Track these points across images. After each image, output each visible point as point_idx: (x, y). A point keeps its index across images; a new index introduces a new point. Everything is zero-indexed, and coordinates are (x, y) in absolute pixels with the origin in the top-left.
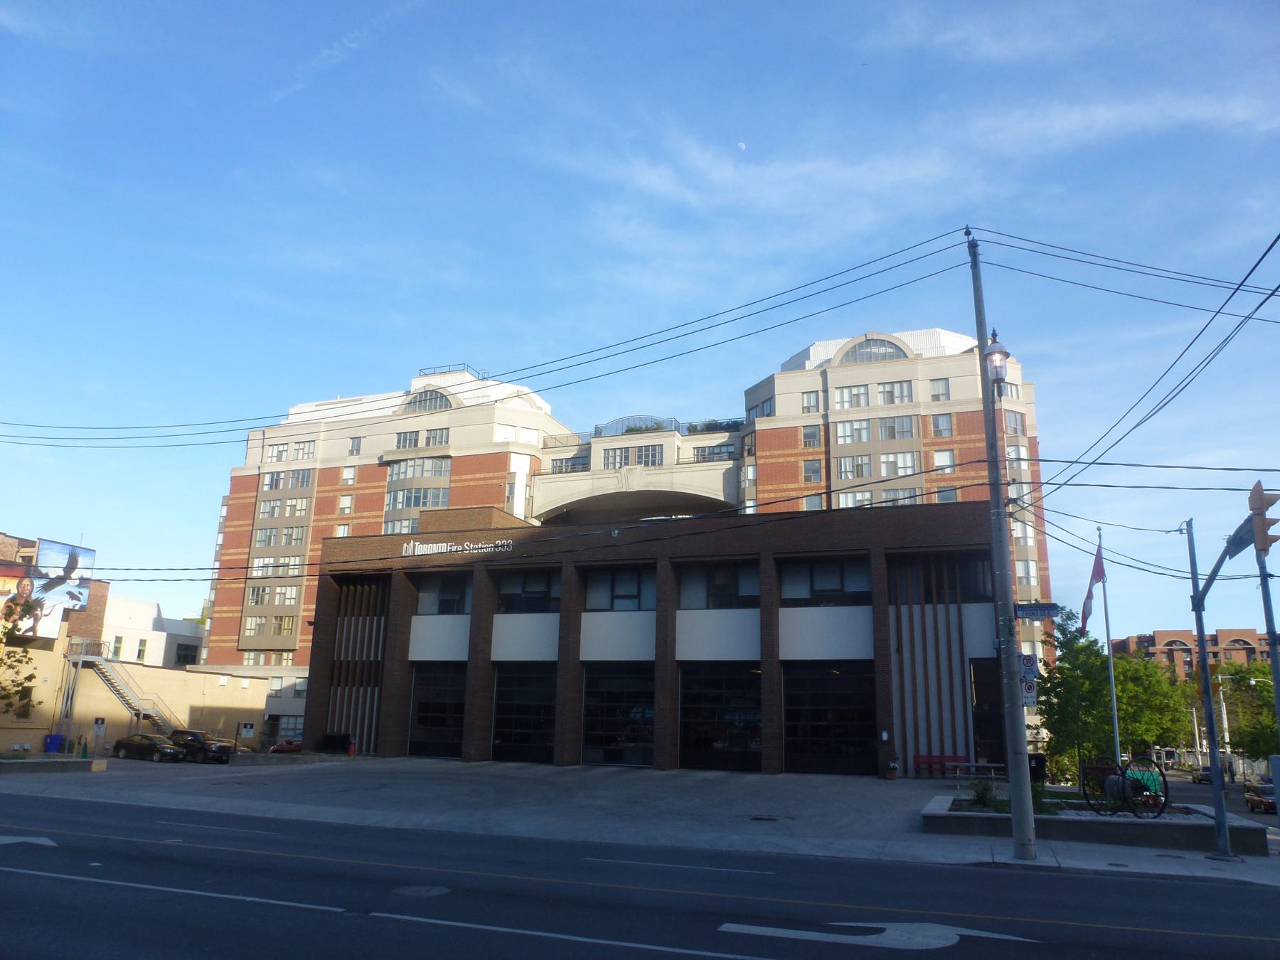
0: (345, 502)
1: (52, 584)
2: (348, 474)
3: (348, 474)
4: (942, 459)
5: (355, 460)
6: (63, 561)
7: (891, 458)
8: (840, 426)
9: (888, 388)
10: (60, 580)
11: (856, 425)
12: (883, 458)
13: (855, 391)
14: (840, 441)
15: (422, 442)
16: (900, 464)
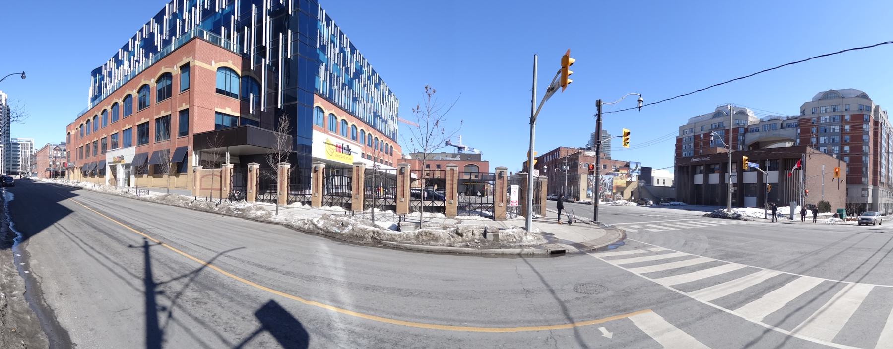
0: (702, 144)
1: (633, 170)
2: (702, 136)
3: (702, 136)
4: (847, 128)
5: (703, 132)
6: (635, 165)
7: (834, 127)
8: (821, 118)
9: (835, 106)
10: (635, 169)
11: (826, 117)
12: (832, 127)
13: (826, 107)
14: (821, 122)
15: (717, 127)
16: (836, 129)
